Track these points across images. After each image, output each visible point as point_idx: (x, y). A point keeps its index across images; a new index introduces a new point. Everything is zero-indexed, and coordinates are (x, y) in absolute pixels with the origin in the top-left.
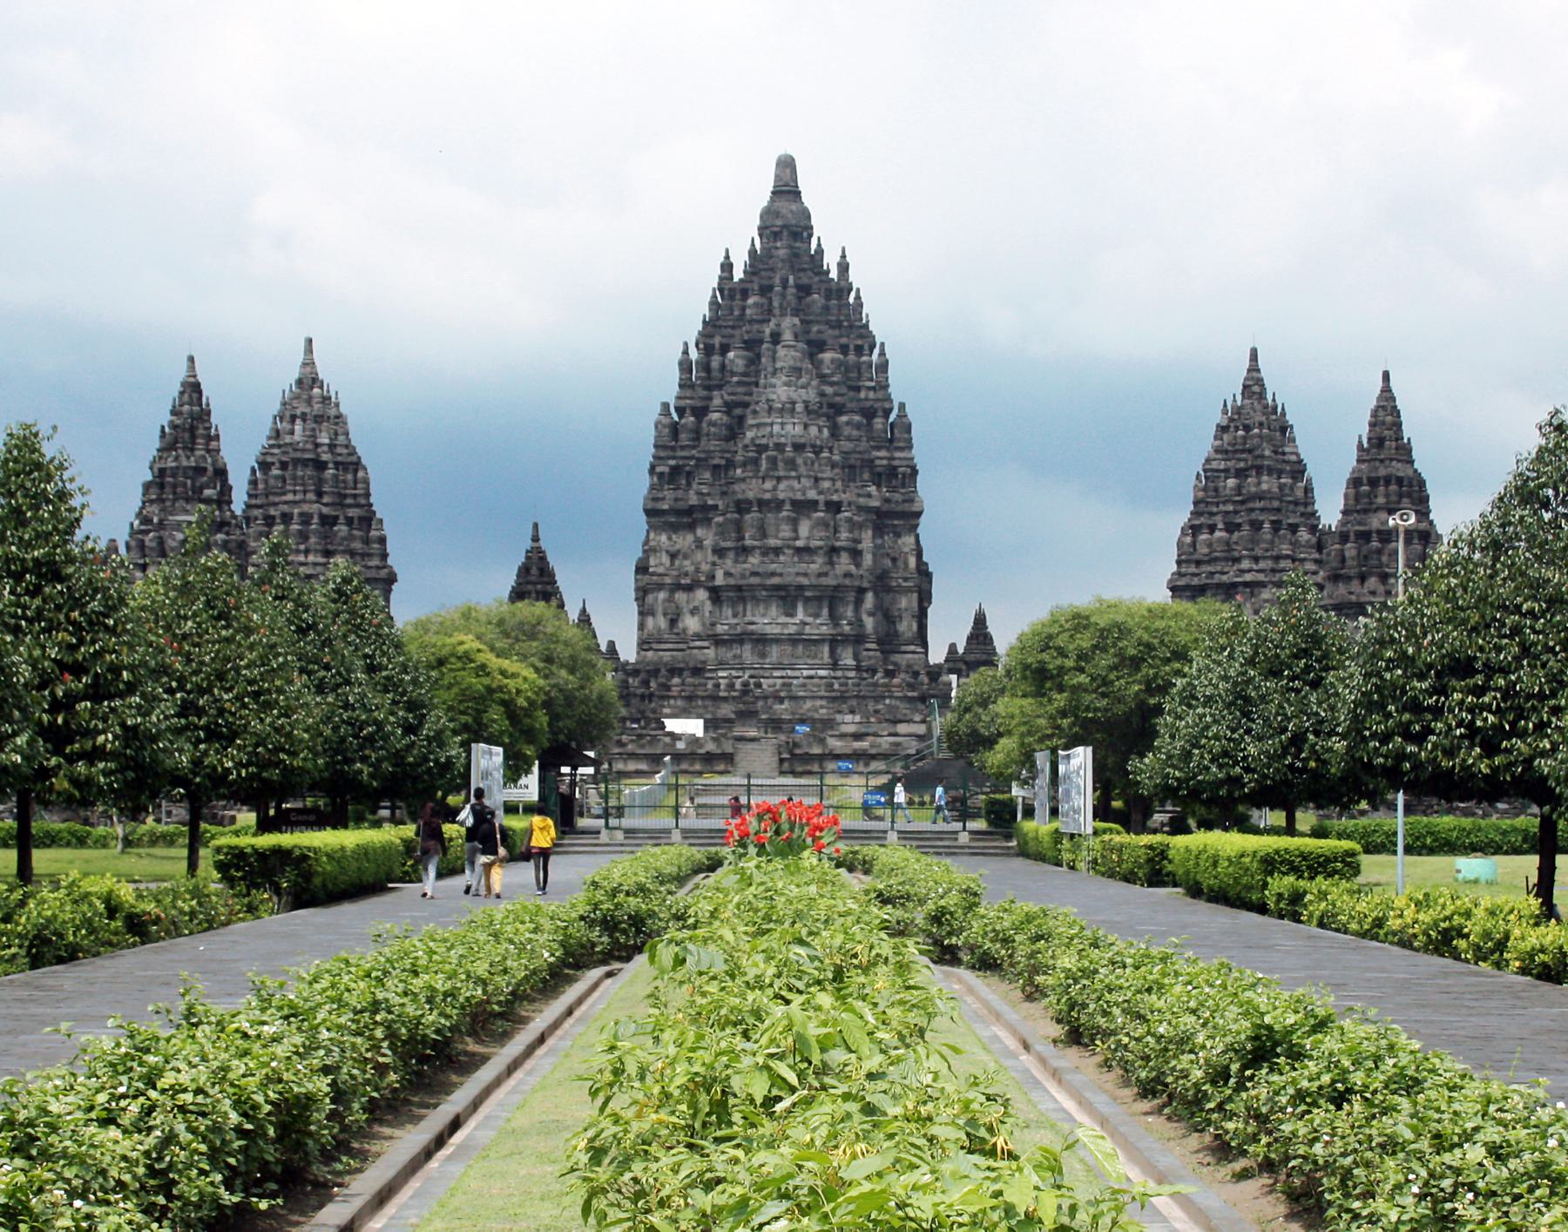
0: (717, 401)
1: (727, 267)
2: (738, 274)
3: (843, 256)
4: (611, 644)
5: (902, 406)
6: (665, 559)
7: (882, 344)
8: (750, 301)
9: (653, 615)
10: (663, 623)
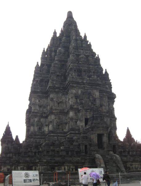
1: (55, 33)
2: (58, 35)
4: (17, 137)
5: (106, 70)
6: (37, 108)
7: (98, 55)
10: (36, 129)
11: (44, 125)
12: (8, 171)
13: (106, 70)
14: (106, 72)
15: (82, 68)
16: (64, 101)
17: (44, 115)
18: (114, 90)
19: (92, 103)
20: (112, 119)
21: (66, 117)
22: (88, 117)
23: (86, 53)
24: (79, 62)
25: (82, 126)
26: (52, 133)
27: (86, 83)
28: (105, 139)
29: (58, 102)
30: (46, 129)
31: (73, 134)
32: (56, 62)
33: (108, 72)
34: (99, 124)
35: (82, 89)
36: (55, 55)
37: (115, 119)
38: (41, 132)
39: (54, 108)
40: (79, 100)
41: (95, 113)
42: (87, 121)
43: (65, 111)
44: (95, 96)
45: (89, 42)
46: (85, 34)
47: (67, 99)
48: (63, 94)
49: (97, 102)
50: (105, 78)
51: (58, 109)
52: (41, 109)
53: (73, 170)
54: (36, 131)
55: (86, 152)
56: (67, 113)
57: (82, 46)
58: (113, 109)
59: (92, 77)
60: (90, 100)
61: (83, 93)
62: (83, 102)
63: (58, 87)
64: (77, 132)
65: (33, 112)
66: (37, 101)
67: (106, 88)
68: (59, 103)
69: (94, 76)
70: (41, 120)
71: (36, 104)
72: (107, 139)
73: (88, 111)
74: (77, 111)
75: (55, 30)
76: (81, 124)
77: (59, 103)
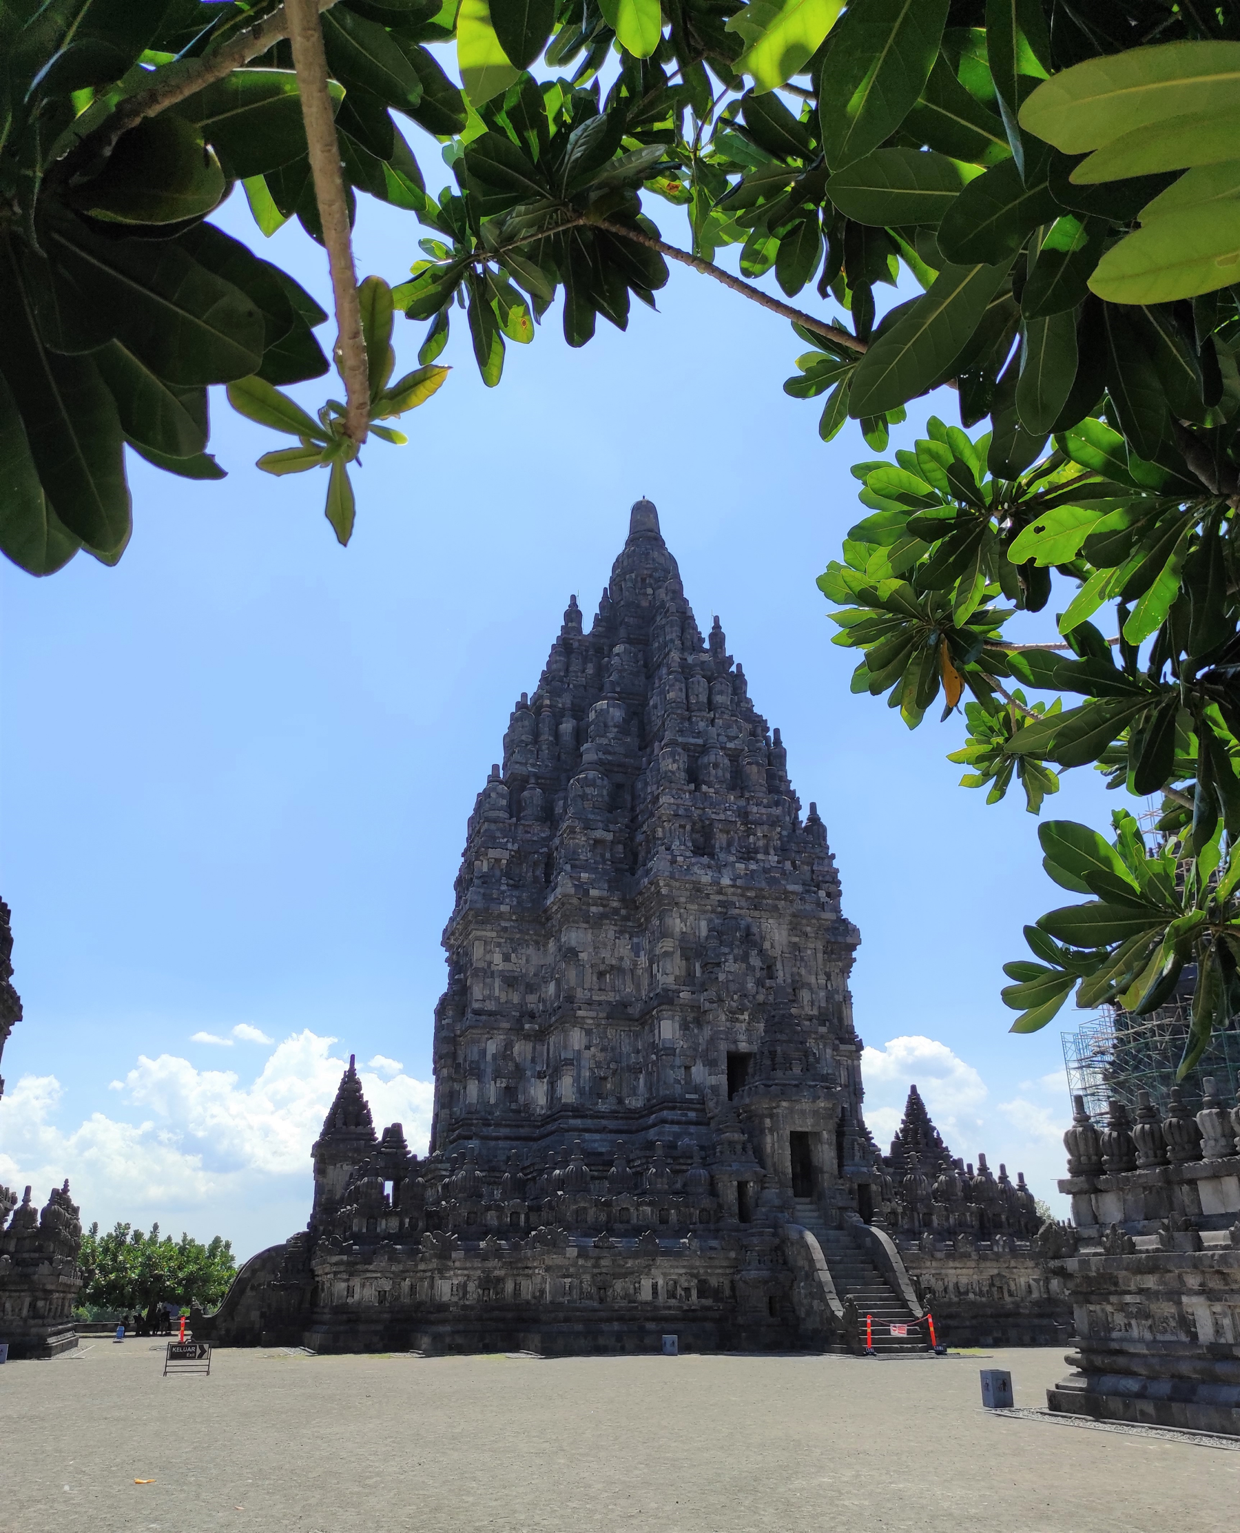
0: (590, 757)
1: (573, 614)
2: (587, 627)
3: (717, 626)
5: (813, 806)
7: (777, 731)
8: (618, 649)
9: (480, 1077)
10: (493, 1091)
11: (528, 1073)
12: (381, 1302)
13: (813, 806)
14: (814, 818)
15: (714, 816)
16: (627, 964)
17: (527, 1026)
18: (850, 909)
19: (760, 983)
20: (842, 1047)
21: (636, 1039)
22: (743, 1047)
23: (731, 739)
24: (697, 788)
25: (715, 1089)
26: (575, 1117)
27: (732, 886)
28: (825, 1155)
29: (602, 968)
30: (538, 1093)
31: (678, 1123)
32: (592, 774)
33: (824, 820)
34: (796, 1086)
35: (709, 915)
36: (580, 735)
37: (853, 1048)
38: (514, 1106)
39: (580, 994)
40: (698, 966)
41: (779, 1036)
42: (737, 1065)
43: (630, 1010)
44: (772, 946)
45: (736, 661)
46: (716, 619)
47: (642, 953)
48: (621, 932)
49: (781, 973)
50: (811, 839)
51: (600, 1003)
52: (516, 999)
53: (688, 1296)
54: (492, 1101)
55: (744, 1215)
56: (645, 1020)
57: (710, 705)
58: (847, 997)
59: (760, 856)
60: (751, 968)
61: (717, 933)
62: (722, 977)
63: (600, 898)
64: (692, 1115)
65: (477, 1013)
66: (497, 958)
67: (822, 906)
68: (601, 975)
69: (767, 853)
70: (516, 1049)
71: (493, 973)
72: (833, 1154)
73: (741, 1017)
74: (695, 1019)
75: (573, 598)
76: (713, 1080)
77: (601, 975)
